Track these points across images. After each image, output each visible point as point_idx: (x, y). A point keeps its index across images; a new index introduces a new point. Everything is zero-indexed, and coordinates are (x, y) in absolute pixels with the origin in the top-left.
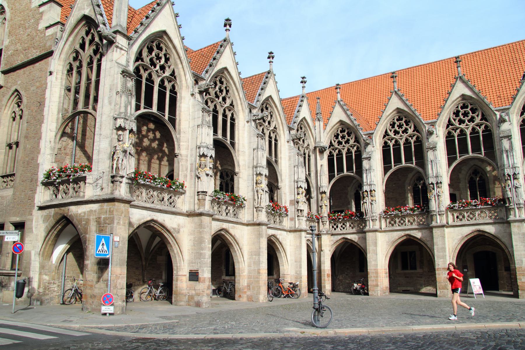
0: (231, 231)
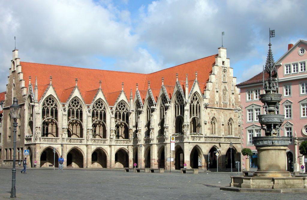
0: (79, 147)
